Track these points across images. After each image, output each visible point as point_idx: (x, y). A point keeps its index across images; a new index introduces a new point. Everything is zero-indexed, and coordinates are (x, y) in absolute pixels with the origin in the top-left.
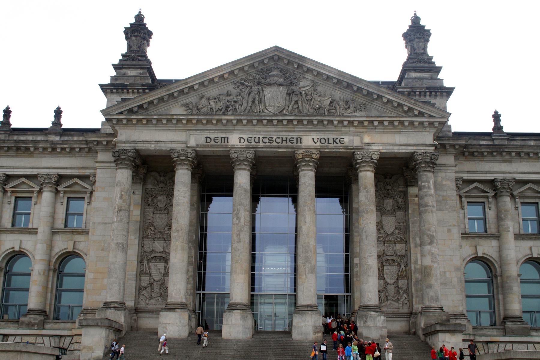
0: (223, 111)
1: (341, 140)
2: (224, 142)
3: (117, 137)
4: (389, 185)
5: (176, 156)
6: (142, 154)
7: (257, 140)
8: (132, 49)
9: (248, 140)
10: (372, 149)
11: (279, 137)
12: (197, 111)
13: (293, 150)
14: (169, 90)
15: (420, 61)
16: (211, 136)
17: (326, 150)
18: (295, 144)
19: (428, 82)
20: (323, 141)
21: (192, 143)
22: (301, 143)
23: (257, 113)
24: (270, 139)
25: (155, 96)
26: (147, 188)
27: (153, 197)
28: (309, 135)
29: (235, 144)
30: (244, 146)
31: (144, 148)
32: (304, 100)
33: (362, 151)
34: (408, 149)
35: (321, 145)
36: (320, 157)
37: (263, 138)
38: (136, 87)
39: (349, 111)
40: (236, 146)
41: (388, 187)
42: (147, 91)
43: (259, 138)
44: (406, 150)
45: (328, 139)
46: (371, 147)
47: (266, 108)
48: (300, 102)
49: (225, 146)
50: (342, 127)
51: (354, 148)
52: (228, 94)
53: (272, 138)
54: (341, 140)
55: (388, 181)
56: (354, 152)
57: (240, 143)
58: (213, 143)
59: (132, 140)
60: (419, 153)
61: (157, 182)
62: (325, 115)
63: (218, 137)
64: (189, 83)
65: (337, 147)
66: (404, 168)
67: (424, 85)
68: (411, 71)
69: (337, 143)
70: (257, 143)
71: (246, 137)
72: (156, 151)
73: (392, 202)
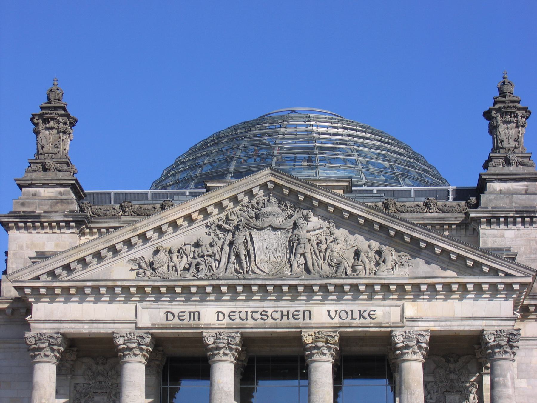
0: (193, 269)
1: (372, 313)
2: (194, 320)
3: (32, 315)
4: (454, 372)
5: (122, 343)
6: (69, 337)
7: (243, 316)
8: (45, 150)
9: (229, 316)
10: (419, 326)
11: (276, 309)
12: (153, 272)
13: (298, 330)
14: (108, 241)
15: (508, 162)
16: (173, 310)
17: (349, 330)
18: (301, 320)
19: (520, 199)
20: (344, 315)
21: (145, 321)
22: (310, 318)
23: (244, 274)
24: (263, 313)
25: (88, 250)
26: (77, 384)
27: (87, 397)
28: (322, 307)
29: (209, 322)
30: (225, 326)
31: (72, 331)
32: (314, 251)
33: (404, 329)
34: (473, 326)
35: (341, 321)
36: (340, 339)
37: (253, 312)
38: (55, 219)
39: (383, 267)
40: (211, 326)
41: (452, 376)
42: (72, 224)
43: (247, 312)
44: (471, 326)
45: (352, 311)
46: (416, 323)
47: (256, 264)
48: (309, 256)
49: (195, 326)
50: (373, 293)
51: (392, 325)
52: (197, 245)
53: (266, 312)
54: (372, 313)
55: (452, 366)
56: (391, 332)
57: (218, 320)
58: (176, 321)
59: (54, 318)
60: (490, 332)
61: (92, 374)
62: (346, 274)
63: (184, 312)
64: (139, 229)
65: (365, 324)
66: (476, 347)
67: (514, 205)
68: (494, 180)
69: (365, 318)
70: (242, 320)
71: (226, 311)
72: (90, 334)
73: (459, 399)
